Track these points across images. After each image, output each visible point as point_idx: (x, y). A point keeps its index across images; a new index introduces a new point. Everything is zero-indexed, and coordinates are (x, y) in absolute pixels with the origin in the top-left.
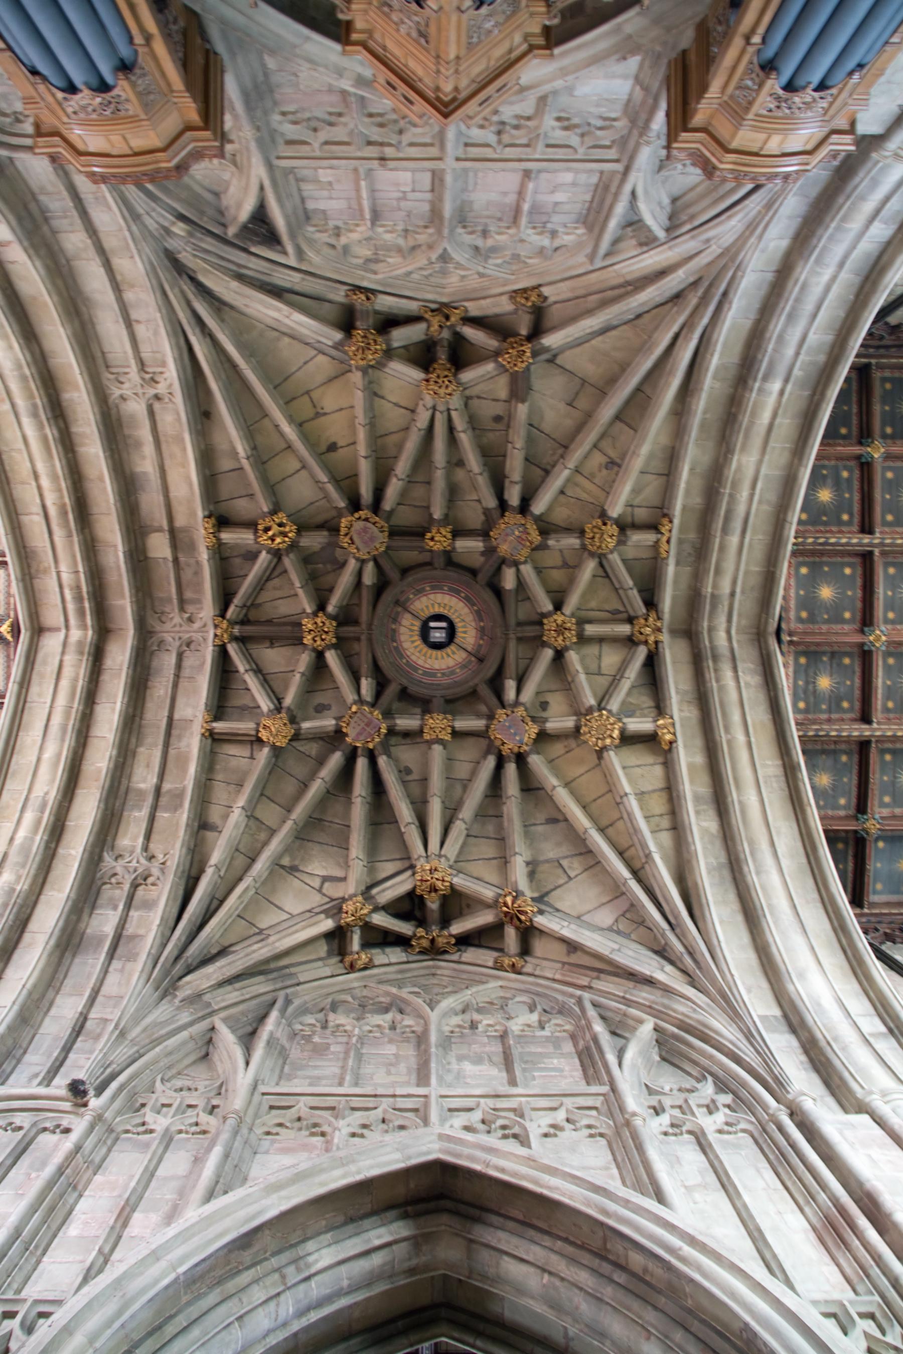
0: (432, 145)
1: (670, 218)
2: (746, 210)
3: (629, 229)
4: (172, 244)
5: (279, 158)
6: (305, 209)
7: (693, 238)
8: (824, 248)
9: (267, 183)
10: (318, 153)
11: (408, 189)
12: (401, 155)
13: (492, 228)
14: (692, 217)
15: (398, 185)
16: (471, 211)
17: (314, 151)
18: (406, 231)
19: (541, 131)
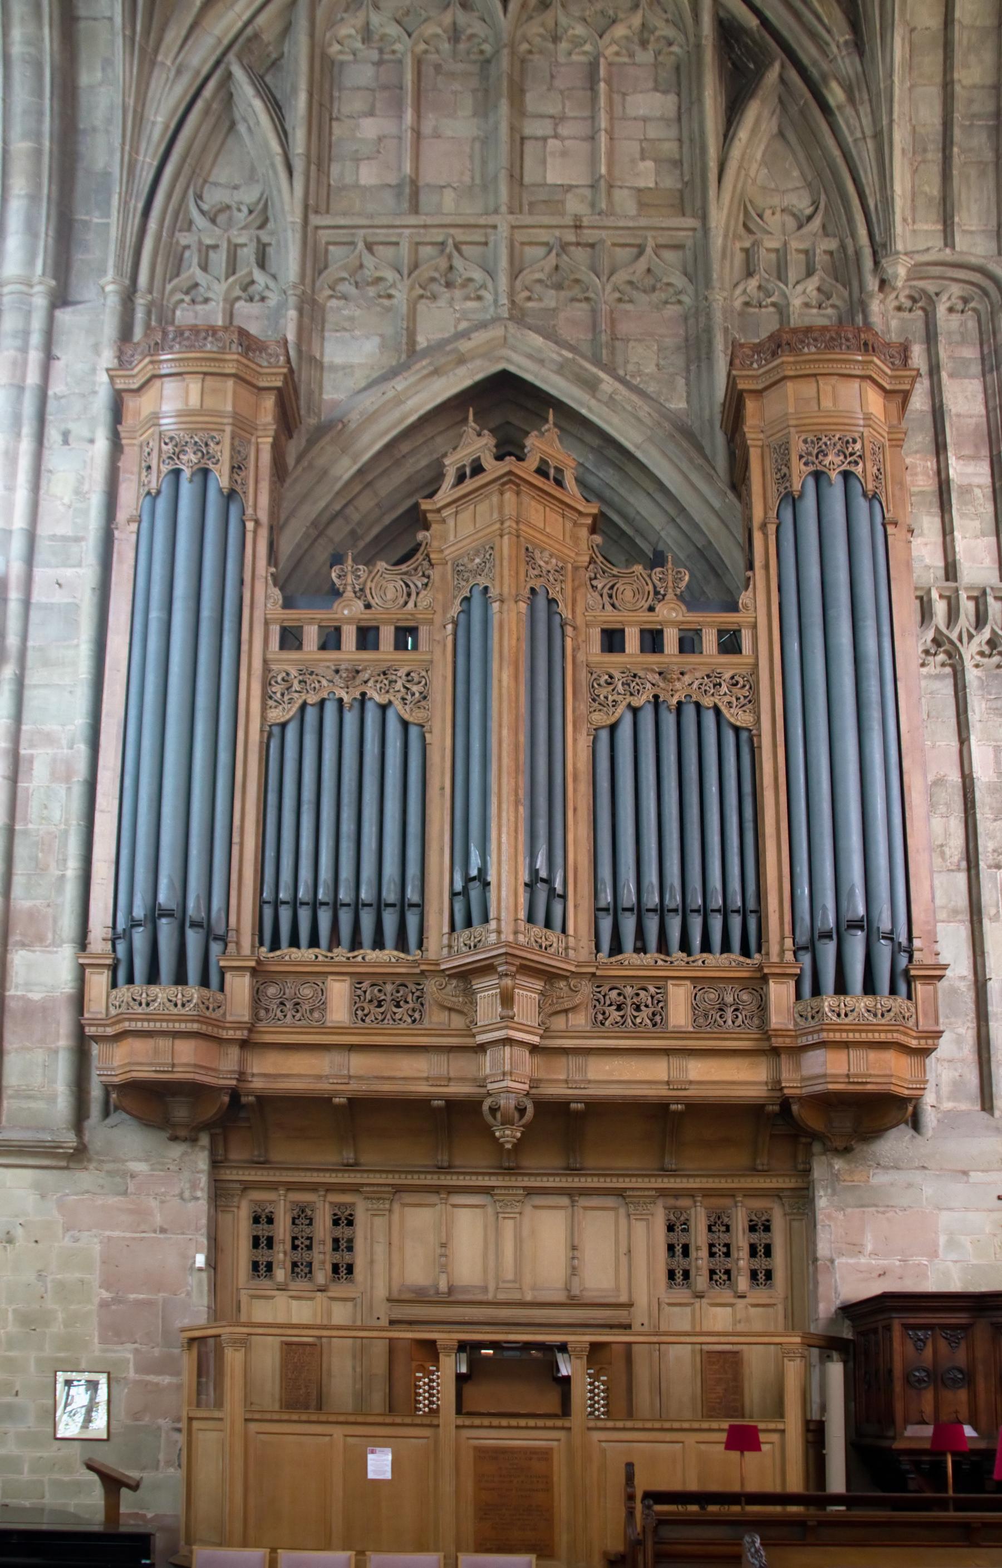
0: (523, 244)
1: (231, 95)
2: (151, 151)
3: (274, 56)
4: (847, 64)
5: (694, 230)
6: (678, 95)
7: (198, 72)
8: (40, 95)
9: (712, 192)
10: (649, 234)
11: (551, 142)
12: (557, 232)
13: (446, 47)
14: (207, 111)
15: (564, 154)
16: (474, 91)
17: (654, 237)
18: (556, 39)
19: (407, 282)
